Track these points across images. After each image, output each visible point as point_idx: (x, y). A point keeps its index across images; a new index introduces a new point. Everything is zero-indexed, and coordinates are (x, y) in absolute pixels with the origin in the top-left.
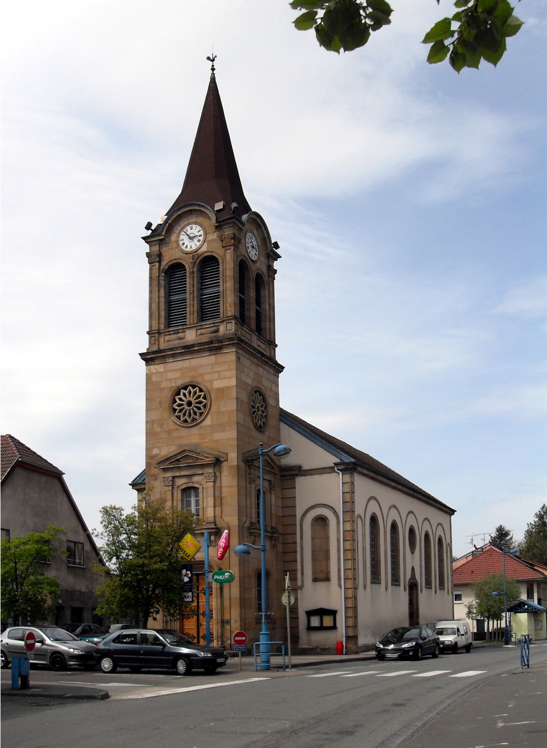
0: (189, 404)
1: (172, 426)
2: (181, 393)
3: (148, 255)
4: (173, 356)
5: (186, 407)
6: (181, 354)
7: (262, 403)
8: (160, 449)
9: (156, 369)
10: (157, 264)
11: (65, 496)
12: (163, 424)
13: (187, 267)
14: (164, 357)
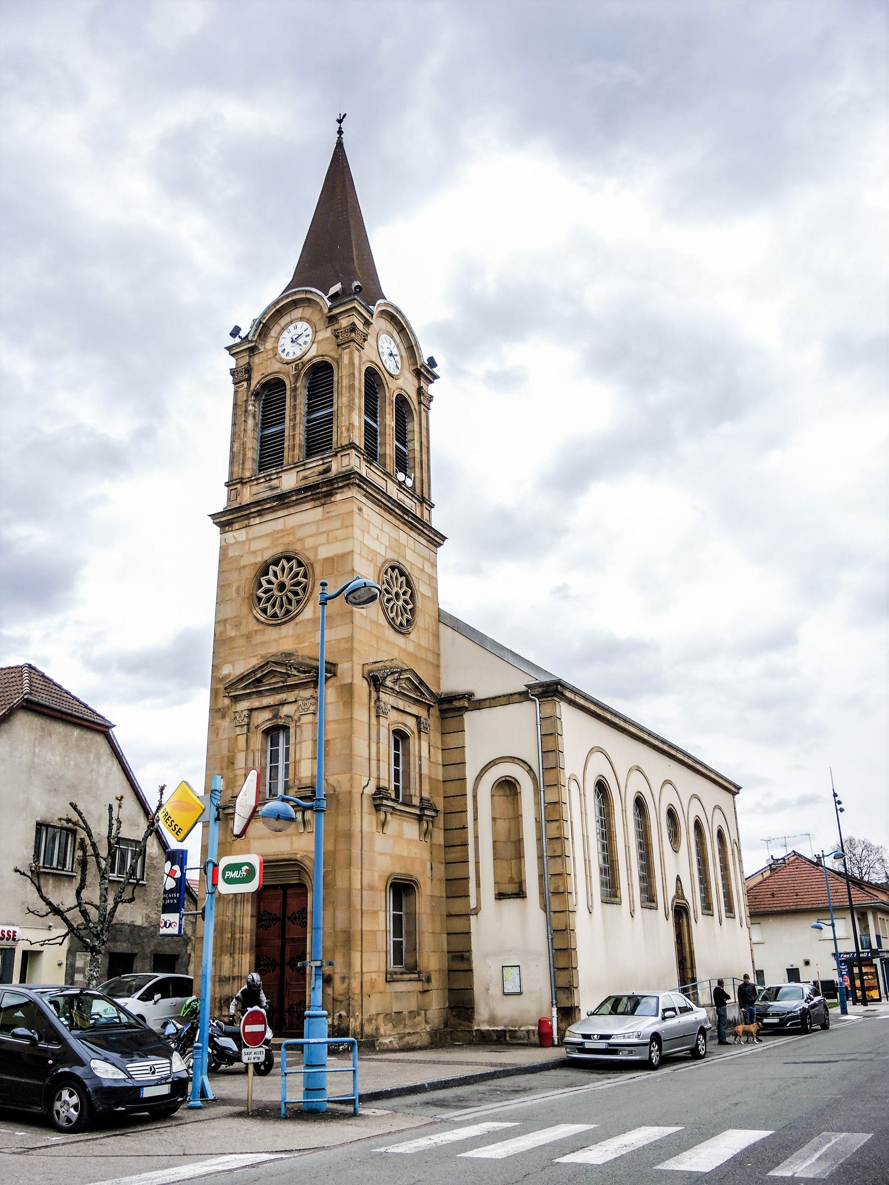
0: (282, 586)
1: (254, 626)
2: (271, 572)
3: (233, 372)
4: (260, 513)
5: (276, 593)
6: (273, 510)
7: (405, 588)
8: (233, 666)
9: (234, 537)
10: (245, 384)
11: (116, 762)
12: (240, 624)
13: (287, 382)
14: (248, 517)
